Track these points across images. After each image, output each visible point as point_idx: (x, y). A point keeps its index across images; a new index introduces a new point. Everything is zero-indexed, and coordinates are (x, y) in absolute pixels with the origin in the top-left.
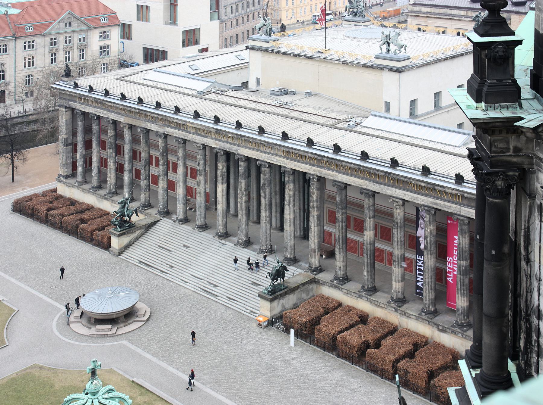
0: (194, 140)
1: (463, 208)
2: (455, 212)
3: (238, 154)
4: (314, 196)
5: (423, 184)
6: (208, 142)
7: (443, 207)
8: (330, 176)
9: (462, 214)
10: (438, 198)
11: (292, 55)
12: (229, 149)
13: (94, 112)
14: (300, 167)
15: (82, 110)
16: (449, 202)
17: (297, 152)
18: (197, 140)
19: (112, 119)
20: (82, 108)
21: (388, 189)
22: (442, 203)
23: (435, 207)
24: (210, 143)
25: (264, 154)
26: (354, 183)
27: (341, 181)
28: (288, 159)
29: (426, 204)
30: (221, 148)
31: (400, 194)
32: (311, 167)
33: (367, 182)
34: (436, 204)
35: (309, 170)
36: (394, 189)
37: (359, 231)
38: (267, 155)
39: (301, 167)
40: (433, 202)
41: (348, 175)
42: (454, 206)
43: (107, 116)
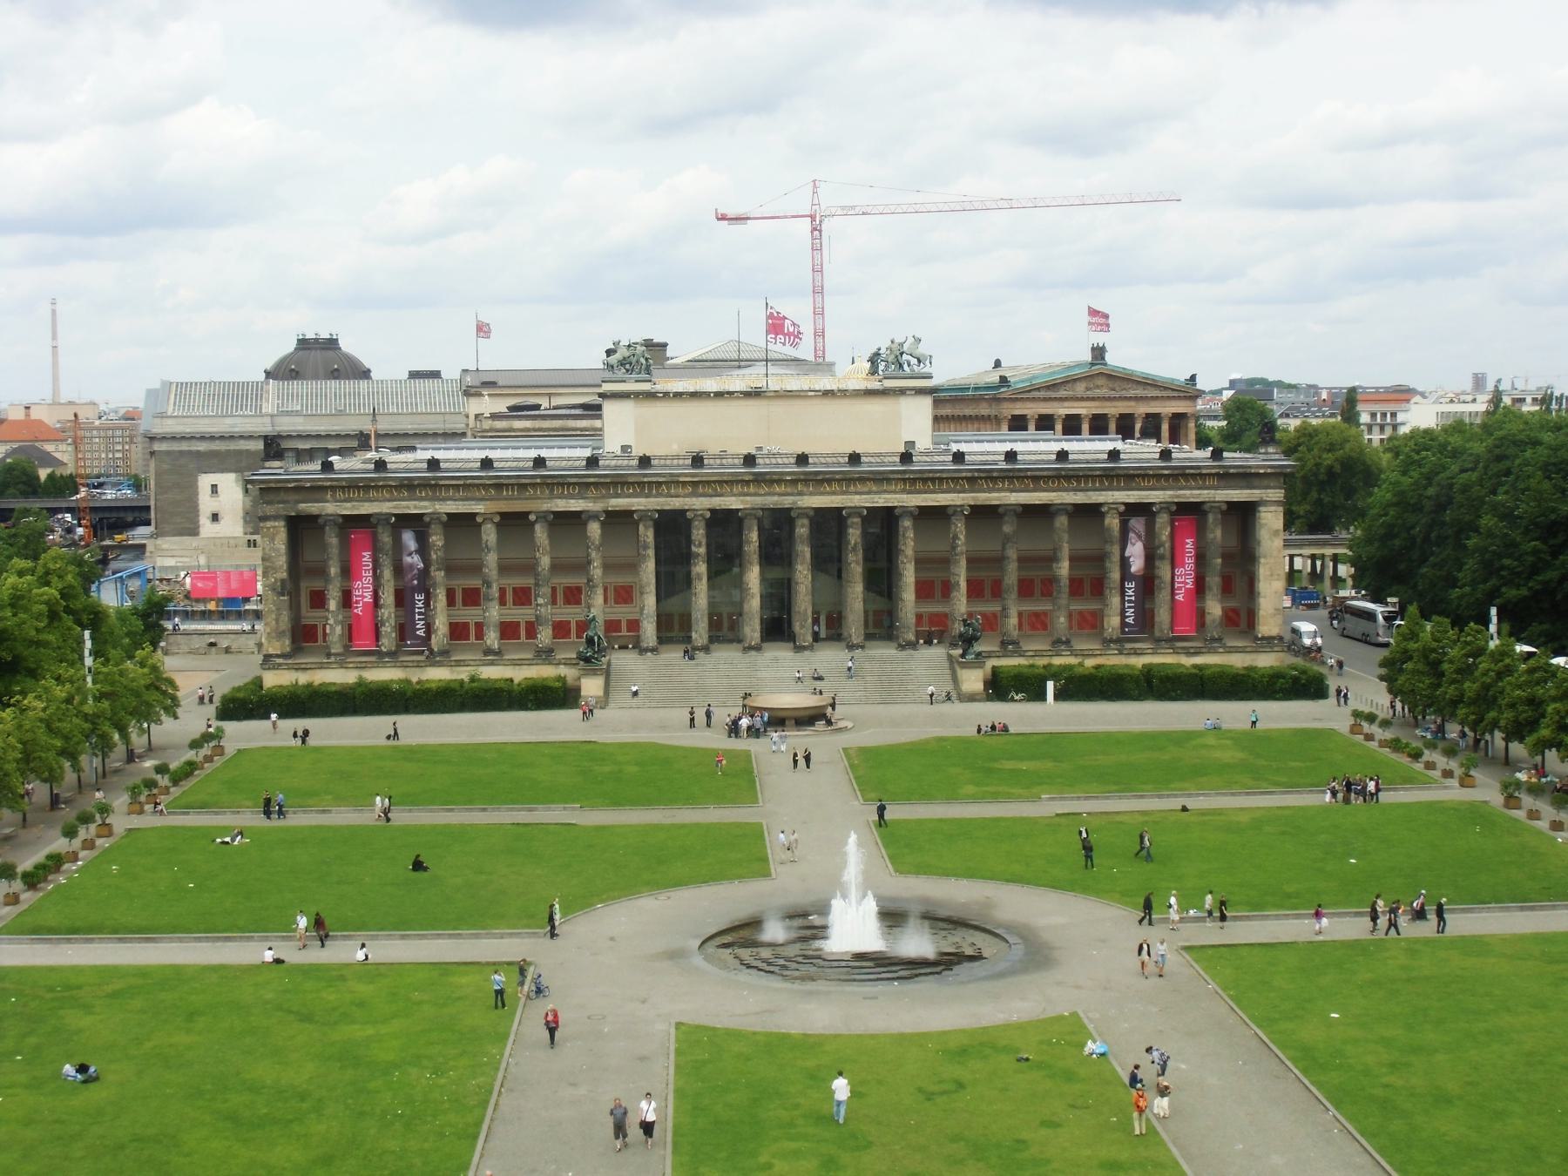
0: (686, 507)
3: (799, 508)
4: (962, 537)
5: (1166, 472)
10: (1181, 489)
16: (1199, 489)
17: (938, 475)
19: (447, 514)
20: (346, 509)
22: (1188, 492)
23: (1176, 500)
25: (857, 497)
33: (1064, 494)
34: (1178, 496)
36: (1110, 493)
42: (1206, 492)
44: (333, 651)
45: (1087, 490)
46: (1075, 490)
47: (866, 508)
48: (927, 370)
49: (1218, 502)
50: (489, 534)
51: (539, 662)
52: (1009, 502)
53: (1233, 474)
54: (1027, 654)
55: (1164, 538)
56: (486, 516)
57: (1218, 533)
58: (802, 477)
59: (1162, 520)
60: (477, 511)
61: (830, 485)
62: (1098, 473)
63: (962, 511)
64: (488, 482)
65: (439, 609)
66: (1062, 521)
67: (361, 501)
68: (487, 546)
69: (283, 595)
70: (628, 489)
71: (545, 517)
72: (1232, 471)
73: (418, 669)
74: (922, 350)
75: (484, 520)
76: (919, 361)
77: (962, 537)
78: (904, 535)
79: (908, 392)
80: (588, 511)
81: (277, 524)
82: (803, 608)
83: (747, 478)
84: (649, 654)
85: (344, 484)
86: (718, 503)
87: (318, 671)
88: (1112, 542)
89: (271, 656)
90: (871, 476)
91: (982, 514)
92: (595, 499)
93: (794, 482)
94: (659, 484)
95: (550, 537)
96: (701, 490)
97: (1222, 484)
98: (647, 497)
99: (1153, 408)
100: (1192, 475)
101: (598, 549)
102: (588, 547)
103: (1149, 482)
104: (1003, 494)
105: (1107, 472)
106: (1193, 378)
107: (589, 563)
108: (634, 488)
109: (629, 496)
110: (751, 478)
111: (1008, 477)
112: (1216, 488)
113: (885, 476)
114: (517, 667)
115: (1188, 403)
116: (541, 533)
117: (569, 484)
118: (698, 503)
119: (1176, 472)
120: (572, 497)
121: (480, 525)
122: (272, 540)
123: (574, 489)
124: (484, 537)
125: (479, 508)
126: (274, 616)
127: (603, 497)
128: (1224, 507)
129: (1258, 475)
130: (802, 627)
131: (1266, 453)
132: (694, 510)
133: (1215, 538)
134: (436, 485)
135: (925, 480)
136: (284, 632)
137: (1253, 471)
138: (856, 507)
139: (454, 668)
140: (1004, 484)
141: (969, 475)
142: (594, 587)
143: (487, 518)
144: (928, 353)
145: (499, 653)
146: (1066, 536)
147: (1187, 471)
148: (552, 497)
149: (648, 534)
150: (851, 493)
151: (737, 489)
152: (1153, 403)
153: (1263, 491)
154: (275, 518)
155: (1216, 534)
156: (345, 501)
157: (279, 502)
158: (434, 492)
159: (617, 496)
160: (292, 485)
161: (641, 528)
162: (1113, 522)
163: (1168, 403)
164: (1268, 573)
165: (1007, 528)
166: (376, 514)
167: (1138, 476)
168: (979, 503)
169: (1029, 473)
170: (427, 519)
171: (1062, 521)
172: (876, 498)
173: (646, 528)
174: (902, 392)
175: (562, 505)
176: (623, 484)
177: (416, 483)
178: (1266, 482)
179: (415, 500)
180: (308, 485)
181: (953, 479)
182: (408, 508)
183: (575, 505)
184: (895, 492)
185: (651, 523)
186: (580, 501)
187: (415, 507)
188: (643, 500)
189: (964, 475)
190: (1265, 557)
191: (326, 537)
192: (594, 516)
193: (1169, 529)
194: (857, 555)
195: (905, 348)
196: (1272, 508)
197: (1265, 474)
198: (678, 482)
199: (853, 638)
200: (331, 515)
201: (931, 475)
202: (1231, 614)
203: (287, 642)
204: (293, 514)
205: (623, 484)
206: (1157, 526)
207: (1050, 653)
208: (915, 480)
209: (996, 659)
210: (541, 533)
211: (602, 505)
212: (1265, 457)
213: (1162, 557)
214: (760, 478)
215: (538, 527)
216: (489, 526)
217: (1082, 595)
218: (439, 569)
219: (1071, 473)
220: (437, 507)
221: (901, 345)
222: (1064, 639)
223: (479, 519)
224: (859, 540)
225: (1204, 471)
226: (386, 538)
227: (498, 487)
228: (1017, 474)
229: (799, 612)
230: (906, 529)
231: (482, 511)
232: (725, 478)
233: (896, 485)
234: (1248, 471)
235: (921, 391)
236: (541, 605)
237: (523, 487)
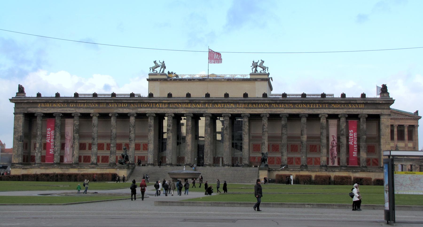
0: (165, 112)
1: (365, 110)
2: (360, 113)
3: (206, 113)
4: (266, 125)
5: (343, 102)
6: (179, 111)
7: (353, 112)
8: (278, 112)
9: (364, 113)
10: (350, 109)
11: (187, 80)
12: (198, 112)
13: (58, 112)
14: (256, 112)
15: (45, 112)
16: (356, 109)
17: (257, 102)
18: (168, 111)
19: (81, 113)
20: (45, 111)
21: (319, 111)
22: (352, 110)
23: (348, 113)
24: (180, 111)
25: (227, 110)
26: (295, 112)
27: (286, 113)
28: (247, 108)
29: (342, 113)
30: (191, 112)
31: (326, 111)
32: (264, 110)
33: (305, 110)
34: (349, 112)
35: (263, 112)
36: (322, 110)
37: (276, 151)
38: (230, 109)
39: (257, 111)
40: (347, 111)
41: (291, 108)
42: (359, 110)
43: (74, 112)
44: (37, 162)
45: (314, 109)
46: (309, 108)
47: (231, 114)
48: (267, 72)
49: (364, 114)
50: (95, 120)
51: (110, 167)
52: (284, 113)
53: (369, 103)
54: (290, 170)
55: (343, 127)
56: (95, 114)
57: (365, 126)
58: (207, 102)
59: (343, 120)
60: (91, 112)
61: (218, 105)
62: (317, 102)
63: (266, 116)
64: (95, 101)
65: (75, 148)
66: (304, 120)
67: (50, 108)
68: (94, 125)
69: (20, 142)
70: (145, 105)
71: (115, 115)
72: (369, 102)
73: (66, 169)
74: (264, 65)
75: (93, 115)
76: (263, 70)
77: (266, 125)
78: (244, 124)
79: (258, 80)
80: (130, 113)
81: (20, 116)
82: (207, 150)
83: (186, 101)
84: (150, 166)
85: (44, 101)
86: (177, 111)
87: (30, 169)
88: (323, 128)
89: (14, 163)
90: (232, 102)
91: (274, 117)
92: (133, 109)
93: (205, 103)
94: (156, 103)
95: (116, 122)
96: (171, 106)
97: (366, 107)
98: (151, 108)
99: (401, 123)
100: (353, 103)
101: (134, 126)
102: (130, 126)
103: (337, 106)
104: (281, 110)
105: (321, 102)
106: (417, 112)
107: (130, 132)
108: (147, 105)
109: (145, 108)
110: (188, 101)
111: (283, 103)
112: (363, 109)
113: (237, 102)
114: (102, 169)
115: (415, 121)
116: (113, 120)
117: (124, 103)
118: (170, 111)
119: (347, 102)
120: (125, 108)
121: (92, 117)
122: (18, 121)
123: (126, 105)
124: (93, 122)
125: (91, 111)
126: (16, 149)
127: (136, 108)
128: (367, 116)
129: (379, 104)
130: (206, 157)
131: (383, 96)
132: (168, 113)
133: (363, 128)
134: (76, 102)
135: (253, 104)
136: (20, 155)
137: (377, 102)
138: (227, 113)
139: (79, 169)
140: (282, 106)
141: (268, 102)
142: (131, 141)
143: (95, 115)
144: (266, 66)
145: (96, 164)
146: (305, 126)
147: (351, 102)
148: (118, 108)
149: (151, 121)
150: (225, 108)
151: (184, 106)
152: (401, 121)
153: (382, 110)
154: (20, 113)
155: (364, 126)
156: (44, 108)
157: (21, 108)
158: (76, 105)
159: (141, 108)
160: (26, 101)
161: (149, 120)
162: (323, 121)
163: (407, 121)
164: (385, 142)
165: (283, 122)
166: (55, 113)
167: (333, 103)
168: (273, 113)
169: (291, 102)
170: (73, 115)
171: (304, 120)
172: (234, 110)
173: (151, 119)
174: (256, 80)
175: (121, 111)
176: (143, 103)
177: (69, 101)
178: (383, 107)
179: (69, 108)
180: (32, 101)
181: (263, 103)
182: (67, 111)
183: (125, 111)
184: (241, 108)
185: (153, 118)
186: (127, 109)
187: (69, 111)
188: (150, 109)
189: (266, 102)
190: (383, 136)
191: (37, 121)
192: (133, 115)
193: (345, 124)
194: (227, 131)
195: (258, 64)
196: (386, 117)
197: (382, 103)
198: (162, 103)
199: (225, 162)
200: (40, 113)
201: (254, 102)
202: (375, 161)
203: (21, 159)
204: (26, 112)
205: (143, 103)
206: (341, 123)
207: (299, 170)
208: (249, 103)
209: (278, 171)
210: (113, 120)
211: (135, 111)
212: (383, 97)
213: (343, 135)
214: (192, 102)
215: (112, 119)
216: (95, 118)
217: (316, 151)
218: (76, 133)
219: (307, 102)
220: (77, 110)
221: (257, 63)
222: (304, 165)
223: (91, 115)
224: (228, 126)
225: (358, 102)
226: (58, 121)
227: (99, 103)
228: (286, 102)
229: (205, 152)
230: (245, 122)
231: (93, 112)
232: (179, 102)
233: (242, 105)
234: (375, 102)
235: (263, 80)
236: (112, 147)
237: (107, 103)
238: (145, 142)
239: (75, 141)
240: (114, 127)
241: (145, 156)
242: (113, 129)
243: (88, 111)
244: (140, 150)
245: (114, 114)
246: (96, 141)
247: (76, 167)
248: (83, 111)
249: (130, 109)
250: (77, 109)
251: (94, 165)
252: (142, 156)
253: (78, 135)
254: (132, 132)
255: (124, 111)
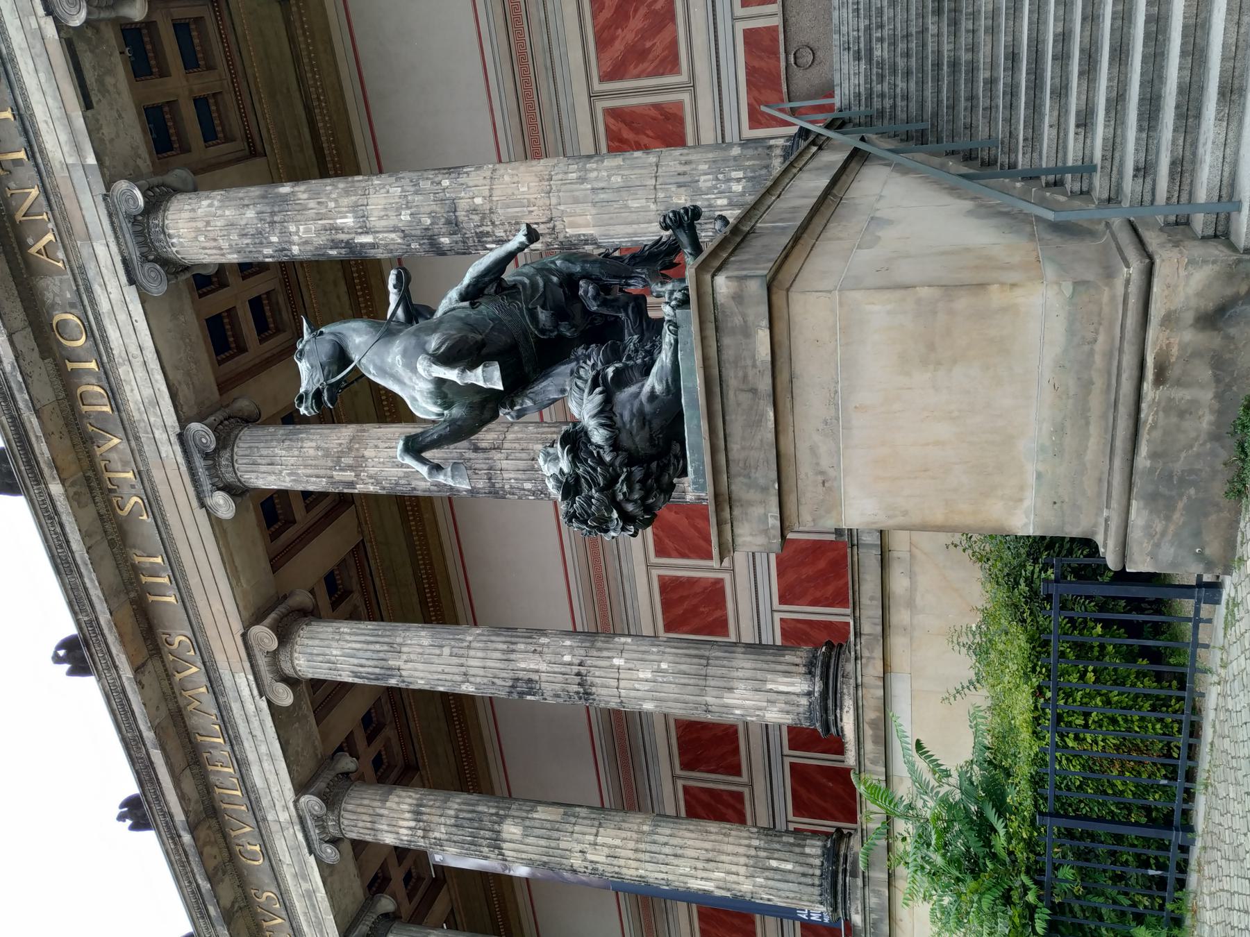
19: (301, 788)
114: (899, 616)
142: (454, 225)
182: (309, 895)
211: (87, 200)
220: (284, 817)
238: (575, 56)
239: (577, 862)
240: (346, 461)
241: (748, 34)
242: (372, 471)
243: (255, 723)
244: (680, 105)
245: (199, 463)
246: (543, 667)
247: (873, 901)
248: (267, 765)
249: (92, 272)
250: (270, 817)
251: (838, 705)
252: (751, 71)
253: (511, 830)
254: (349, 221)
255: (134, 350)
